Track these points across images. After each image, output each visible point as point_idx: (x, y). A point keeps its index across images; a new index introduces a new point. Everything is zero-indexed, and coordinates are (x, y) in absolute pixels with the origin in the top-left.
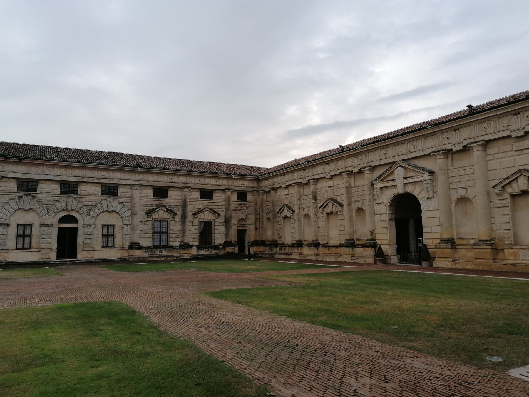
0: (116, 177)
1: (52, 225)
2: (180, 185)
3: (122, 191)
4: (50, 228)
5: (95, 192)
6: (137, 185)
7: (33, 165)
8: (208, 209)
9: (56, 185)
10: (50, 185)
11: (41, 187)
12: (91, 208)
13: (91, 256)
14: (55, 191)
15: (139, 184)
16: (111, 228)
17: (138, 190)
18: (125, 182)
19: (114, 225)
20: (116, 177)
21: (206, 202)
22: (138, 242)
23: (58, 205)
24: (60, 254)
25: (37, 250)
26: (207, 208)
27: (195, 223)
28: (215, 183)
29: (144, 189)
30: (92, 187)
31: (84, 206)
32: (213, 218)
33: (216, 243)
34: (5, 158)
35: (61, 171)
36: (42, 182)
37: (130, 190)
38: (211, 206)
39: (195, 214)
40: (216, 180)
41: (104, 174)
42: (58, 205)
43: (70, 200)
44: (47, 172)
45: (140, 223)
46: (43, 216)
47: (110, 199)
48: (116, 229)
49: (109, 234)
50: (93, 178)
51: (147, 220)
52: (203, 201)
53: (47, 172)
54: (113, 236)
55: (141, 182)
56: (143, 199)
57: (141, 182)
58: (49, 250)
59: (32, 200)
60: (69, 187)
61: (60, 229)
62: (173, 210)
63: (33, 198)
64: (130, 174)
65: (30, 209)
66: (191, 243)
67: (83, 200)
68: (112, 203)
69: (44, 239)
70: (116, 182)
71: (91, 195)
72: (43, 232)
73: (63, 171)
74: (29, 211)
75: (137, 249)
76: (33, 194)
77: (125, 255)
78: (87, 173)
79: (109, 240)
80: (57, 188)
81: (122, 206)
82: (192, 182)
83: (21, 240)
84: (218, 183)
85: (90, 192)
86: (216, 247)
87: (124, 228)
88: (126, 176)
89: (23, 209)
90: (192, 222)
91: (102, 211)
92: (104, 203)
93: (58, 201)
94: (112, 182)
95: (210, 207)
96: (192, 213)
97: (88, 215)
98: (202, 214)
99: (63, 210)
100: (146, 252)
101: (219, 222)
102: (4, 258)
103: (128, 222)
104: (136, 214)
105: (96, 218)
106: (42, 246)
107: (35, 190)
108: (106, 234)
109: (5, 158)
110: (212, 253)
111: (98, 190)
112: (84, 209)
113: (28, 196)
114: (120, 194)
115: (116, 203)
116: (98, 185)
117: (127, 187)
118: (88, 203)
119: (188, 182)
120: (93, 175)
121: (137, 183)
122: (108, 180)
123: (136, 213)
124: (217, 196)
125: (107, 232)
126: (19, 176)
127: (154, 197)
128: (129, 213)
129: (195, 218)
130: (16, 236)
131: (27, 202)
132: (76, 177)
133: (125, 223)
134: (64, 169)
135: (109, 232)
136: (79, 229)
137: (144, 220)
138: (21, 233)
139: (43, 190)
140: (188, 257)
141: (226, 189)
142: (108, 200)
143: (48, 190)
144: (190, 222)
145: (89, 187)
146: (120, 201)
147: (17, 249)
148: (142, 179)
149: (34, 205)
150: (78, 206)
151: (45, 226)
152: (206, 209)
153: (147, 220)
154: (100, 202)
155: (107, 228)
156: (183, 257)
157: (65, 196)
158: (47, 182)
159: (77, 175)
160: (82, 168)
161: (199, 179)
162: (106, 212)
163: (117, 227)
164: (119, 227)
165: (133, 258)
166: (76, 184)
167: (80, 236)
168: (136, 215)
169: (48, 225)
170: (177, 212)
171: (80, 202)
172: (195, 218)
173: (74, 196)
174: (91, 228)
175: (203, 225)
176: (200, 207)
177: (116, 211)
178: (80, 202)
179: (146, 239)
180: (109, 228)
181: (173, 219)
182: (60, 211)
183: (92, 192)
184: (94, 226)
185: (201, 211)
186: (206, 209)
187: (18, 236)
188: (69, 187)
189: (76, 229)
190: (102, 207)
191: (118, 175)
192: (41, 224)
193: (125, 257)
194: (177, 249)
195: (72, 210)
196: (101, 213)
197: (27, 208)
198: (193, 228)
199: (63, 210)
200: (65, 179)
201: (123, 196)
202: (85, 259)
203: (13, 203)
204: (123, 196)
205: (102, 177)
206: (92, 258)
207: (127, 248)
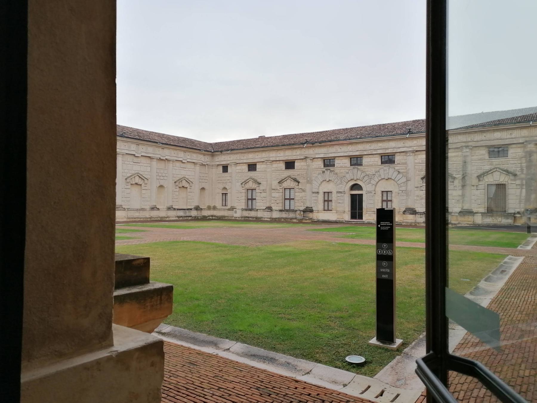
0: (390, 146)
1: (344, 192)
2: (459, 145)
3: (397, 158)
4: (343, 195)
5: (375, 162)
6: (410, 151)
7: (330, 145)
8: (497, 170)
9: (346, 160)
10: (343, 160)
11: (337, 162)
12: (371, 177)
13: (372, 219)
14: (346, 165)
15: (412, 150)
16: (390, 194)
17: (411, 156)
18: (399, 150)
19: (391, 191)
20: (390, 146)
21: (497, 161)
22: (412, 207)
23: (347, 176)
24: (353, 216)
25: (335, 212)
26: (496, 168)
27: (480, 187)
28: (509, 136)
29: (420, 154)
30: (372, 158)
31: (367, 175)
32: (506, 179)
33: (511, 211)
34: (313, 144)
35: (348, 148)
36: (337, 158)
37: (405, 157)
38: (504, 166)
39: (479, 177)
40: (510, 132)
41: (380, 145)
42: (347, 176)
43: (356, 170)
44: (339, 150)
45: (416, 189)
46: (338, 185)
47: (386, 167)
48: (393, 195)
49: (388, 199)
50: (372, 151)
51: (423, 186)
52: (491, 160)
53: (339, 150)
54: (391, 201)
55: (415, 148)
56: (418, 165)
57: (415, 148)
58: (342, 212)
59: (330, 173)
60: (357, 160)
61: (352, 196)
62: (452, 173)
63: (331, 171)
64: (404, 141)
65: (330, 180)
66: (475, 210)
67: (366, 170)
68: (388, 170)
69: (339, 203)
70: (391, 151)
71: (372, 165)
72: (338, 197)
73: (350, 148)
74: (330, 182)
75: (410, 214)
76: (332, 168)
77: (401, 220)
78: (367, 146)
79: (388, 204)
80: (347, 162)
81: (397, 173)
82: (475, 140)
83: (326, 203)
84: (513, 136)
85: (371, 163)
86: (513, 216)
87: (400, 194)
88: (400, 144)
89: (326, 180)
90: (477, 186)
91: (380, 179)
92: (382, 172)
93: (348, 173)
94: (387, 151)
95: (501, 167)
96: (476, 175)
97: (370, 183)
98: (490, 176)
99: (352, 180)
100: (421, 217)
101: (517, 185)
102: (316, 216)
103: (403, 188)
104: (409, 180)
105: (376, 186)
106: (339, 209)
107: (334, 165)
108: (386, 199)
109: (313, 144)
110: (502, 223)
111: (378, 160)
112: (366, 178)
113: (328, 170)
114: (397, 162)
115: (391, 170)
116: (377, 155)
117: (402, 154)
118: (369, 172)
119: (469, 140)
120: (372, 148)
121: (410, 149)
122: (384, 150)
123: (409, 179)
124: (512, 152)
125: (386, 197)
126: (322, 156)
127: (324, 167)
128: (404, 180)
129: (479, 180)
130: (392, 201)
131: (328, 175)
132: (359, 152)
133: (401, 189)
134: (350, 146)
135: (388, 197)
136: (363, 195)
137: (419, 186)
138: (385, 198)
139: (338, 165)
140: (467, 225)
141: (526, 141)
142: (385, 168)
143: (341, 164)
144: (473, 186)
145: (370, 158)
146: (396, 168)
147: (324, 210)
148: (416, 145)
149: (332, 177)
150: (362, 176)
151: (339, 193)
152: (495, 170)
153: (423, 186)
154: (379, 171)
155: (386, 194)
156: (460, 225)
157: (352, 168)
158: (341, 158)
159: (360, 149)
160: (362, 142)
161: (485, 134)
162: (384, 180)
163: (394, 193)
164: (396, 192)
165: (405, 222)
166: (360, 157)
167: (364, 201)
168: (410, 182)
169: (341, 192)
170: (457, 176)
171: (363, 172)
172: (479, 180)
173: (359, 167)
174: (372, 194)
175: (493, 189)
176: (487, 168)
177: (392, 178)
178: (363, 172)
179: (422, 205)
180: (388, 194)
181: (452, 184)
182: (349, 181)
183: (373, 163)
184: (374, 192)
185: (487, 172)
186: (495, 170)
187: (325, 201)
188: (357, 160)
189: (362, 195)
190: (380, 176)
191: (392, 144)
192: (337, 192)
193: (400, 221)
194: (457, 216)
195: (357, 179)
196: (380, 180)
197: (328, 180)
198: (478, 192)
199: (352, 180)
200: (351, 154)
201: (399, 164)
202: (367, 220)
203: (320, 176)
204: (399, 164)
205: (379, 148)
206: (373, 221)
207: (402, 213)
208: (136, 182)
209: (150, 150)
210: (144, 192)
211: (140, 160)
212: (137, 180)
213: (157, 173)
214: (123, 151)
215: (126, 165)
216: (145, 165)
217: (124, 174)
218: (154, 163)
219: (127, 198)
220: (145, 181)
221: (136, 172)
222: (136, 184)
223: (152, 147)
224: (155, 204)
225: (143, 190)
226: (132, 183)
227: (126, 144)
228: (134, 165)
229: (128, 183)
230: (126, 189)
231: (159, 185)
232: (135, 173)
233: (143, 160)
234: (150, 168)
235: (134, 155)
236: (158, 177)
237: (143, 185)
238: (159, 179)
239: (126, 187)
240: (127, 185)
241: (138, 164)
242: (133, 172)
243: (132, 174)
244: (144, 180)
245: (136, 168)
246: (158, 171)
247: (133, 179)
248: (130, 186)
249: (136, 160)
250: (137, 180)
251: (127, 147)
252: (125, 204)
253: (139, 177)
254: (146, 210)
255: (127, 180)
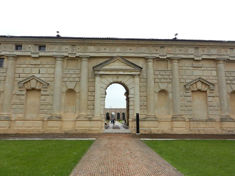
208: (198, 88)
209: (214, 53)
210: (210, 99)
211: (202, 64)
212: (200, 86)
213: (226, 76)
214: (178, 56)
215: (183, 71)
216: (208, 69)
217: (182, 80)
218: (222, 66)
219: (187, 107)
220: (210, 87)
221: (197, 78)
222: (199, 91)
223: (217, 49)
224: (227, 114)
225: (208, 97)
226: (192, 89)
227: (181, 49)
228: (193, 71)
229: (188, 89)
230: (186, 97)
231: (231, 91)
232: (196, 79)
233: (206, 64)
234: (216, 71)
235: (193, 59)
236: (228, 82)
237: (208, 91)
238: (230, 84)
239: (186, 94)
240: (186, 92)
241: (199, 69)
242: (194, 77)
243: (193, 80)
244: (209, 85)
245: (198, 73)
246: (228, 74)
247: (194, 85)
248: (190, 93)
249: (196, 64)
250: (200, 86)
251: (183, 51)
252: (186, 114)
253: (202, 83)
254: (214, 121)
255: (186, 87)
